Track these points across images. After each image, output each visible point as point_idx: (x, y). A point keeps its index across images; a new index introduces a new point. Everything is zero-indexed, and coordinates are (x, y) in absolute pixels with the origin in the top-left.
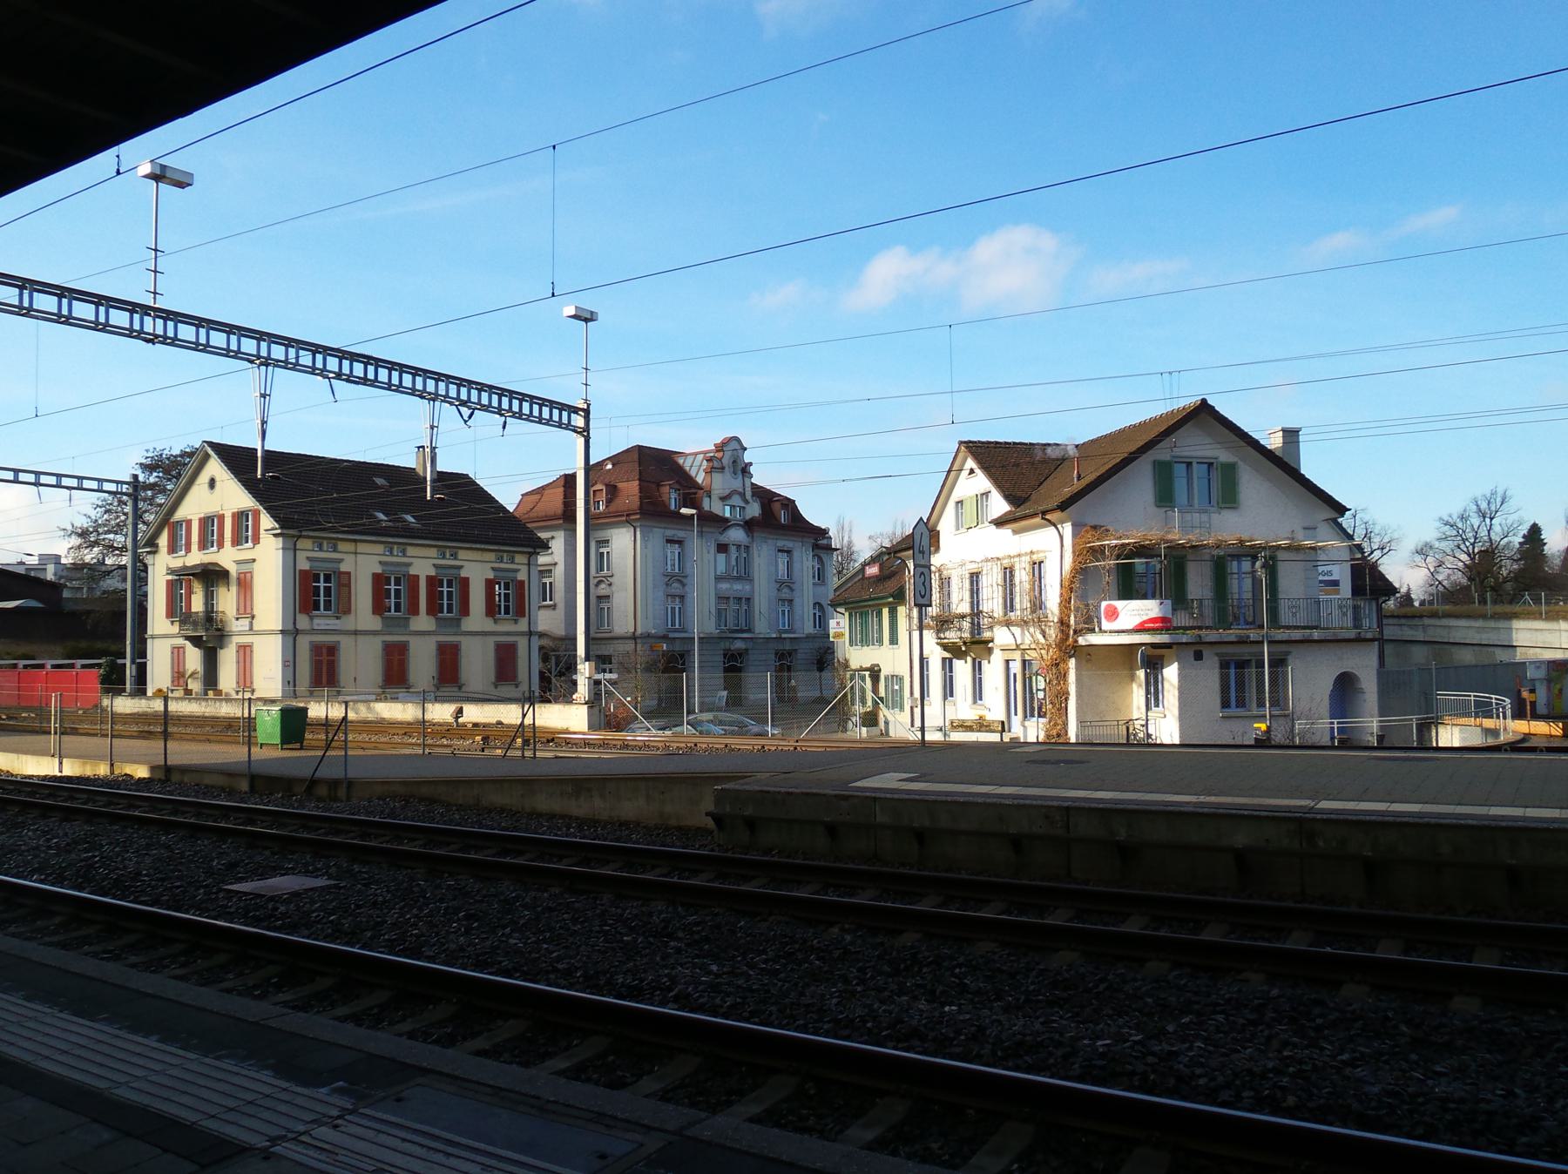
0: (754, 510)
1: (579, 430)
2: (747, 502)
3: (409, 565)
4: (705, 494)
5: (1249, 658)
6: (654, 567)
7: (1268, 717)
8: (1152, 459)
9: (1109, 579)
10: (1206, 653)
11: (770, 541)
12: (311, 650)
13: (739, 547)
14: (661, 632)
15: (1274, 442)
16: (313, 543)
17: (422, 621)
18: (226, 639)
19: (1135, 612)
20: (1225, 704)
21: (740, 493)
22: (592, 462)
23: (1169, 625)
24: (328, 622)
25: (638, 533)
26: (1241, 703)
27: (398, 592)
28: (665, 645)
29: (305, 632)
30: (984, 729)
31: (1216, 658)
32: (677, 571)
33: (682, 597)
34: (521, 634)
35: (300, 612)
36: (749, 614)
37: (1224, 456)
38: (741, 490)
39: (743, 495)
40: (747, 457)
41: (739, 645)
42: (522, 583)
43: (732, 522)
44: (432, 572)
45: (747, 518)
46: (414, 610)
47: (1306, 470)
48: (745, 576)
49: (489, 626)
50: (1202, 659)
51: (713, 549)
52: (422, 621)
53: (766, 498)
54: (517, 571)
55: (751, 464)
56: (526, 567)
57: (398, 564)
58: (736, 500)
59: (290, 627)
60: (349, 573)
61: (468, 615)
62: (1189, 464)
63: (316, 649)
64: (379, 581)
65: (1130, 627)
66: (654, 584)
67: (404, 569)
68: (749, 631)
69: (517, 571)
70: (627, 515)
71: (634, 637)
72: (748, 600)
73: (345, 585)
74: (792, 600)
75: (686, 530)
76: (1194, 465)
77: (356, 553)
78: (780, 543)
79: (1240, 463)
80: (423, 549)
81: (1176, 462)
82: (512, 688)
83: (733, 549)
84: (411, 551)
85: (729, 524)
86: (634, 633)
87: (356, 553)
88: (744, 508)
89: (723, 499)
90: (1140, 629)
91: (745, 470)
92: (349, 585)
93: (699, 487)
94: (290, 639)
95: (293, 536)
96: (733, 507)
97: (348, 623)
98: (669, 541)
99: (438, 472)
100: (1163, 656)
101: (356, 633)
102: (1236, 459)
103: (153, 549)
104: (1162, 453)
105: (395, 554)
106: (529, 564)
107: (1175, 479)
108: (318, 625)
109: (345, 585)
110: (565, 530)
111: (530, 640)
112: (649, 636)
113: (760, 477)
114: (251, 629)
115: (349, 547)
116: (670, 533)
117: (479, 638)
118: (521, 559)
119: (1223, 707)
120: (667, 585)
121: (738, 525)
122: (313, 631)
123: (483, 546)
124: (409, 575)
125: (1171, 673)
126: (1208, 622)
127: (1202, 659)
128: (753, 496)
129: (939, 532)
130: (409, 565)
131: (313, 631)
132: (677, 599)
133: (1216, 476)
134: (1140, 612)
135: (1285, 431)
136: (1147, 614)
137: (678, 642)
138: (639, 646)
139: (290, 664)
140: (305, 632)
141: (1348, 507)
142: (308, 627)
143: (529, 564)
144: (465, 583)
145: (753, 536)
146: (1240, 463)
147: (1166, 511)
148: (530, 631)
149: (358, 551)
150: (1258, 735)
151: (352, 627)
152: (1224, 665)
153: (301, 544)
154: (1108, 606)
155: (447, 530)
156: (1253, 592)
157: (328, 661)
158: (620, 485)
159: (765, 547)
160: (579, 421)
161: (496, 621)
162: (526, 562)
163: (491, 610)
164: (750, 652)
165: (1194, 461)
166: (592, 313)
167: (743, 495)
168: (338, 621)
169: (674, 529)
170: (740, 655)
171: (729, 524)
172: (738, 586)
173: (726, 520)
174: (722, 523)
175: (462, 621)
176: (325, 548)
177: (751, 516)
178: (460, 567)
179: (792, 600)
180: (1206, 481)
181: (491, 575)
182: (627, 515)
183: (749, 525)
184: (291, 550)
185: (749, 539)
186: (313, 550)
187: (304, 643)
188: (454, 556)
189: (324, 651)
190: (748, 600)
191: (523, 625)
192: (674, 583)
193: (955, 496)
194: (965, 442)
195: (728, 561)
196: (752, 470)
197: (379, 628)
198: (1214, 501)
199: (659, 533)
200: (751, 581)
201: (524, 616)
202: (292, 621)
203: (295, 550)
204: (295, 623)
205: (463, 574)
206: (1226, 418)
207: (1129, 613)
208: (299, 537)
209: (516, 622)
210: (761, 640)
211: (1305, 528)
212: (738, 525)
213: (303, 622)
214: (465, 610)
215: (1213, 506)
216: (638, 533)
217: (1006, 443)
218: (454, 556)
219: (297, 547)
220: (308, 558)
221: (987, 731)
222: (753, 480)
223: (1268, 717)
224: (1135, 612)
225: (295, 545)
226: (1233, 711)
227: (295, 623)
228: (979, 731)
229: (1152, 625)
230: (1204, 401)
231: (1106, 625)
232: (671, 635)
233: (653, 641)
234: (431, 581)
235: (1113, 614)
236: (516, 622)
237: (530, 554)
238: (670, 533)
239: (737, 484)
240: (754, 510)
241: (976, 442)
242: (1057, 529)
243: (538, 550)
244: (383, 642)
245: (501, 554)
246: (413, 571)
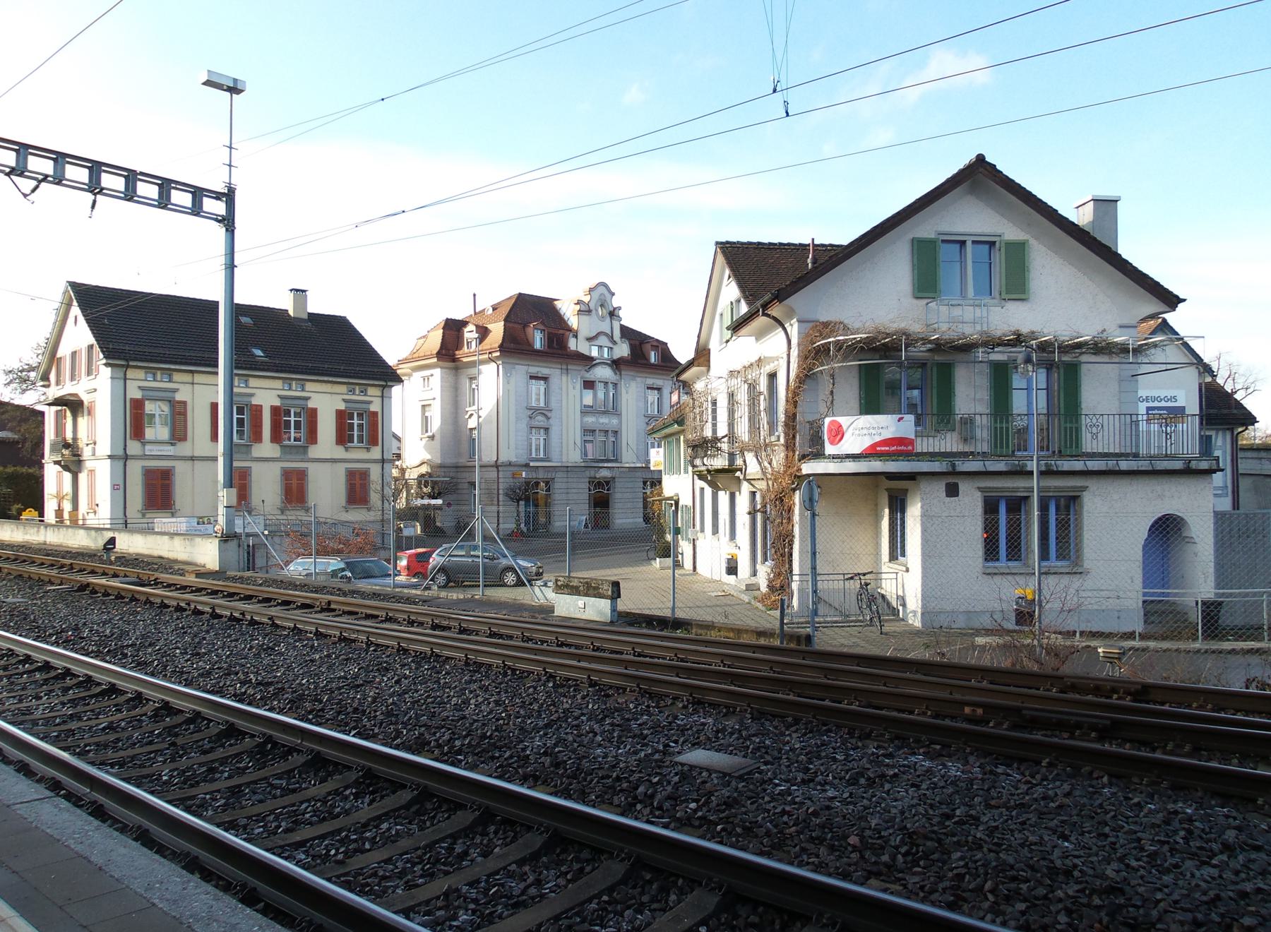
0: (623, 350)
1: (220, 218)
2: (615, 343)
3: (252, 395)
4: (571, 334)
5: (1025, 494)
6: (516, 401)
7: (1037, 574)
8: (911, 237)
9: (850, 390)
10: (964, 486)
11: (639, 379)
12: (347, 476)
13: (606, 383)
14: (523, 460)
15: (1082, 217)
16: (146, 373)
17: (267, 448)
18: (83, 463)
19: (865, 431)
20: (991, 551)
21: (606, 334)
22: (477, 311)
23: (910, 448)
24: (162, 448)
25: (501, 367)
26: (1015, 551)
27: (360, 426)
28: (524, 473)
29: (135, 457)
30: (591, 592)
31: (979, 494)
33: (547, 430)
34: (375, 461)
35: (131, 438)
36: (616, 446)
37: (1010, 232)
38: (609, 332)
39: (611, 338)
40: (616, 302)
41: (605, 473)
42: (375, 414)
43: (598, 361)
44: (277, 403)
45: (615, 358)
46: (257, 437)
47: (1125, 249)
48: (613, 409)
49: (340, 452)
50: (957, 495)
51: (579, 385)
52: (267, 448)
53: (638, 342)
54: (370, 402)
55: (620, 308)
56: (380, 399)
57: (165, 390)
58: (603, 341)
59: (121, 452)
60: (185, 403)
61: (316, 443)
62: (963, 243)
63: (149, 474)
64: (342, 418)
65: (857, 451)
66: (516, 418)
67: (364, 406)
68: (616, 461)
69: (370, 402)
70: (490, 353)
71: (497, 466)
72: (616, 432)
73: (180, 414)
74: (548, 429)
75: (550, 368)
76: (969, 244)
77: (193, 384)
78: (650, 381)
79: (1033, 242)
80: (317, 384)
81: (943, 241)
82: (364, 512)
83: (600, 387)
84: (309, 386)
85: (594, 362)
86: (496, 461)
87: (193, 384)
88: (611, 348)
89: (589, 339)
90: (871, 453)
91: (613, 314)
92: (185, 414)
93: (570, 330)
94: (121, 463)
95: (122, 366)
96: (600, 347)
97: (183, 449)
98: (532, 377)
99: (309, 313)
100: (907, 490)
101: (192, 459)
102: (1025, 238)
103: (46, 383)
104: (926, 228)
105: (159, 379)
106: (382, 397)
107: (942, 265)
108: (151, 450)
109: (180, 414)
110: (441, 368)
111: (125, 465)
112: (510, 464)
113: (630, 319)
114: (94, 455)
115: (187, 378)
116: (534, 370)
117: (328, 465)
118: (377, 392)
119: (986, 559)
120: (530, 418)
121: (607, 364)
122: (144, 457)
123: (331, 379)
124: (251, 405)
125: (914, 512)
126: (984, 447)
127: (957, 495)
128: (622, 337)
129: (709, 350)
130: (252, 395)
131: (144, 457)
132: (542, 430)
133: (999, 258)
134: (871, 431)
135: (1096, 201)
136: (880, 434)
137: (541, 470)
138: (501, 473)
139: (121, 487)
140: (135, 457)
141: (1181, 297)
142: (140, 453)
143: (382, 397)
144: (312, 414)
145: (621, 374)
146: (1033, 242)
147: (927, 304)
149: (195, 382)
150: (1021, 606)
151: (189, 454)
152: (990, 507)
153: (131, 373)
154: (832, 422)
155: (111, 347)
156: (1048, 409)
157: (361, 484)
158: (489, 326)
159: (633, 384)
160: (219, 208)
161: (347, 449)
162: (380, 394)
163: (343, 437)
164: (616, 480)
165: (969, 240)
166: (235, 80)
167: (611, 338)
168: (172, 448)
169: (538, 366)
170: (607, 483)
171: (594, 362)
172: (604, 420)
173: (592, 359)
174: (587, 361)
175: (253, 448)
176: (294, 388)
177: (619, 356)
178: (307, 399)
179: (548, 429)
180: (988, 265)
181: (342, 406)
182: (490, 353)
183: (617, 364)
184: (122, 380)
185: (618, 377)
186: (283, 389)
187: (135, 469)
188: (364, 392)
189: (357, 476)
190: (616, 432)
191: (376, 453)
192: (539, 418)
193: (719, 311)
194: (722, 243)
195: (595, 396)
196: (621, 313)
197: (278, 456)
198: (995, 292)
199: (522, 370)
200: (620, 415)
201: (377, 445)
202: (122, 447)
203: (125, 379)
204: (125, 449)
205: (311, 405)
206: (1013, 181)
207: (857, 432)
208: (128, 366)
209: (368, 450)
210: (624, 469)
211: (1121, 327)
212: (607, 364)
213: (134, 447)
214: (312, 437)
215: (994, 298)
216: (501, 367)
217: (770, 244)
218: (364, 392)
219: (128, 377)
220: (343, 400)
221: (595, 596)
222: (622, 323)
223: (1037, 574)
224: (865, 431)
225: (125, 374)
226: (1002, 564)
227: (125, 449)
228: (587, 595)
229: (887, 448)
230: (980, 159)
231: (830, 449)
232: (532, 464)
233: (516, 468)
234: (275, 411)
235: (838, 434)
236: (368, 450)
237: (384, 387)
238: (534, 370)
239: (605, 326)
240: (623, 350)
241: (734, 243)
242: (785, 329)
243: (389, 384)
244: (143, 467)
245: (353, 386)
246: (255, 401)
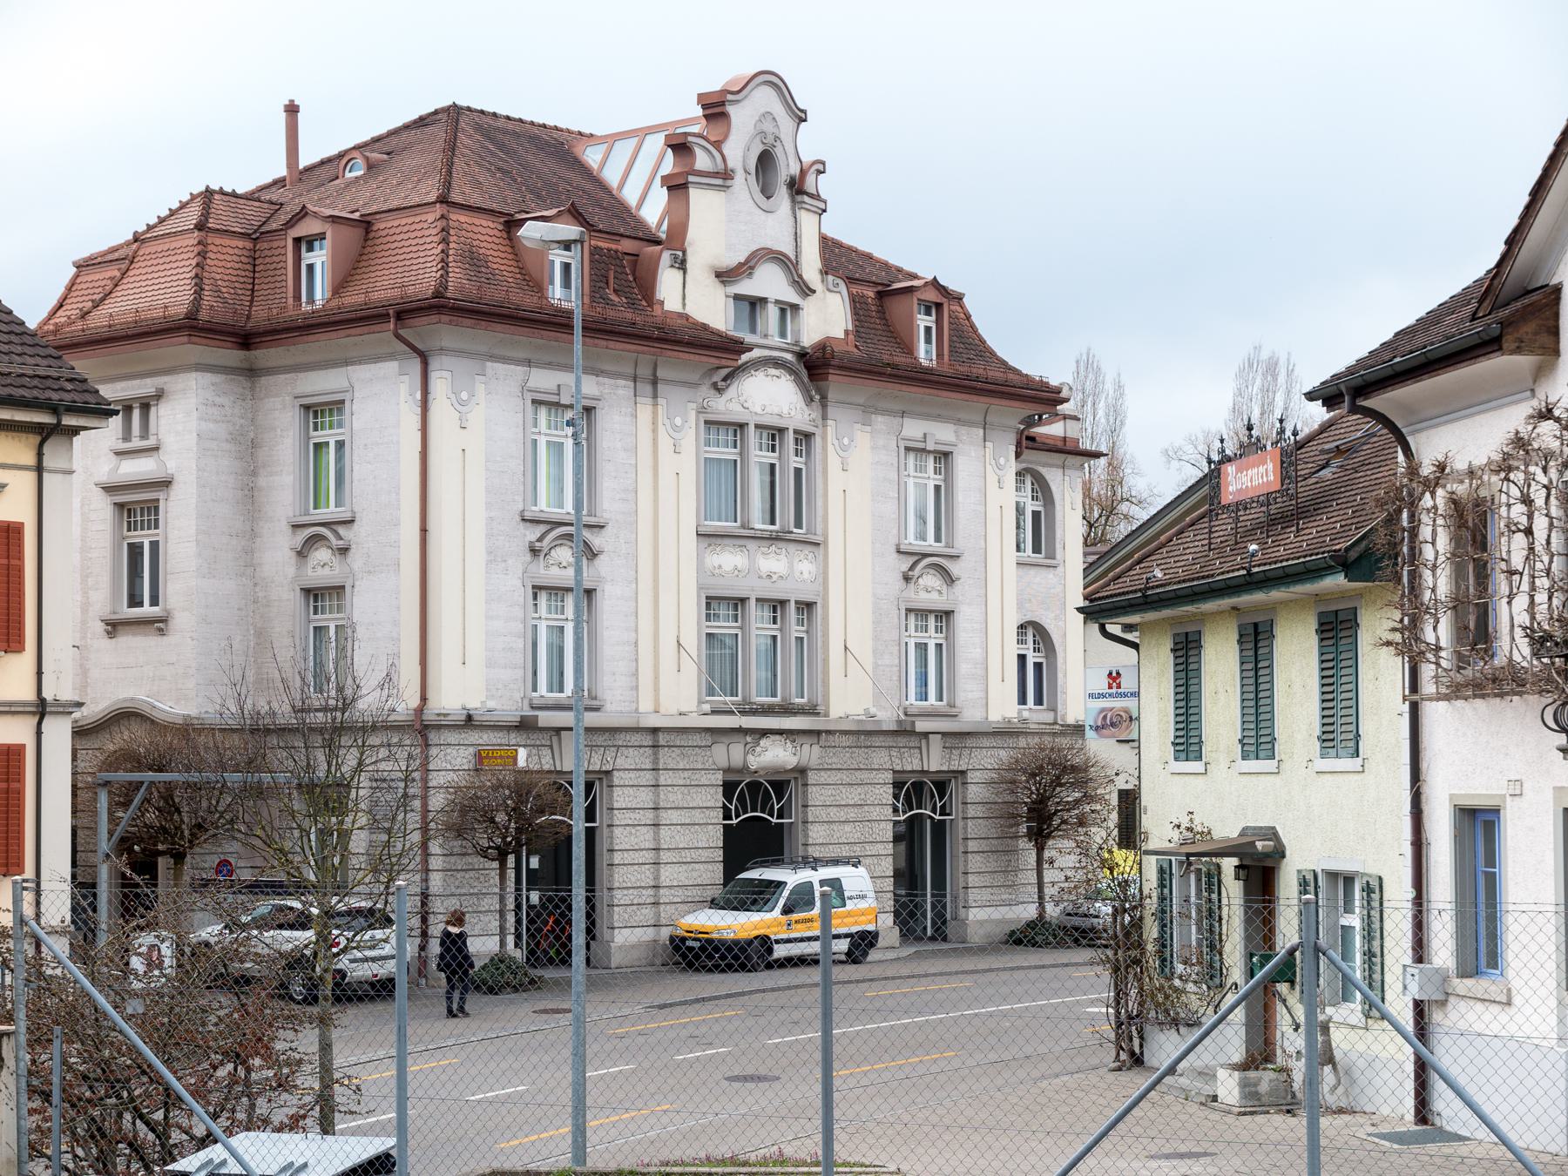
2: (806, 290)
11: (880, 421)
13: (775, 434)
21: (779, 258)
22: (304, 162)
32: (569, 507)
39: (790, 265)
40: (809, 144)
43: (756, 353)
56: (31, 477)
68: (811, 711)
72: (806, 607)
74: (948, 614)
78: (914, 429)
86: (420, 711)
88: (795, 308)
106: (39, 469)
120: (534, 552)
121: (777, 363)
128: (825, 272)
143: (39, 469)
145: (824, 398)
148: (42, 702)
164: (812, 777)
167: (790, 265)
171: (745, 357)
185: (816, 414)
196: (824, 185)
237: (44, 433)
243: (69, 421)
